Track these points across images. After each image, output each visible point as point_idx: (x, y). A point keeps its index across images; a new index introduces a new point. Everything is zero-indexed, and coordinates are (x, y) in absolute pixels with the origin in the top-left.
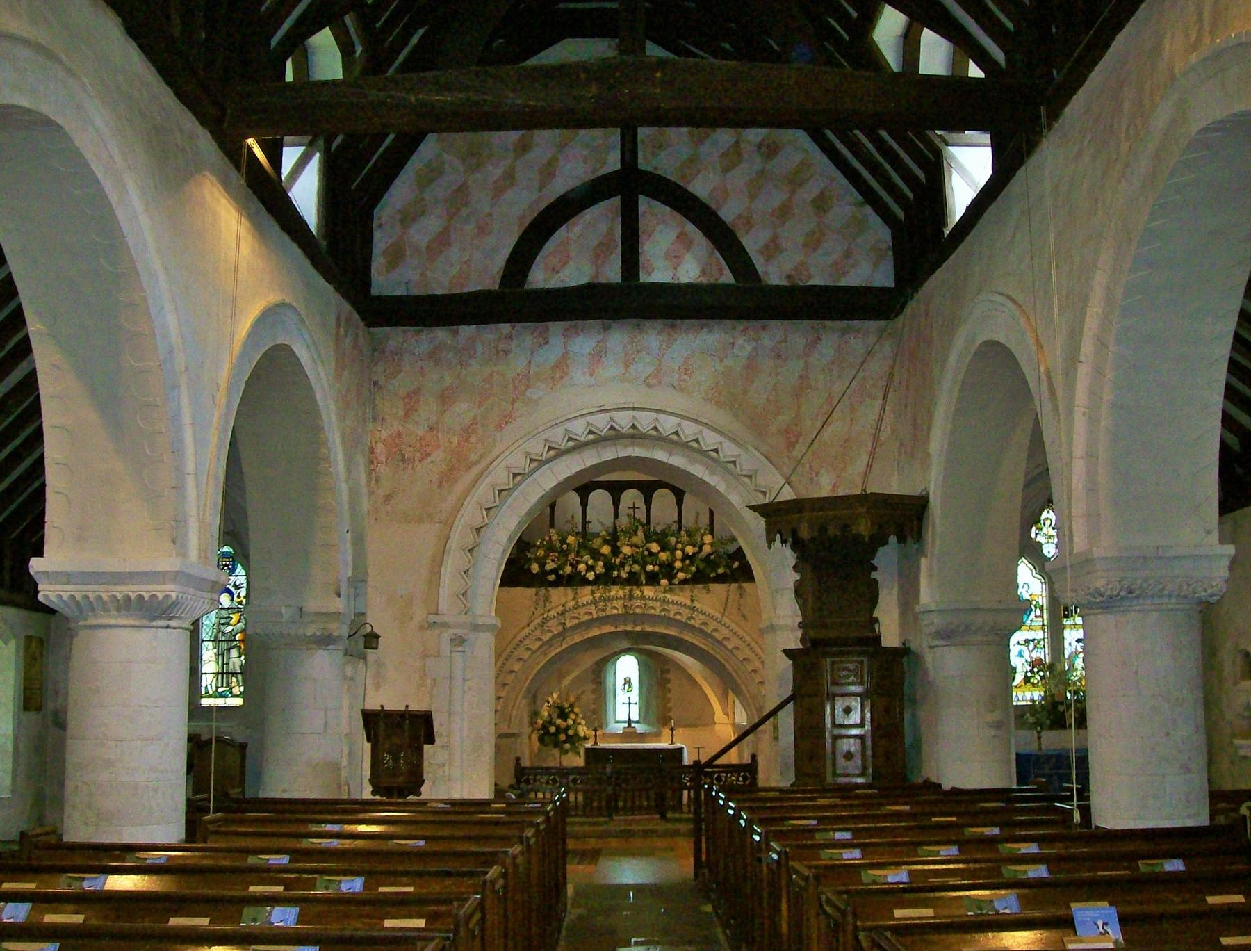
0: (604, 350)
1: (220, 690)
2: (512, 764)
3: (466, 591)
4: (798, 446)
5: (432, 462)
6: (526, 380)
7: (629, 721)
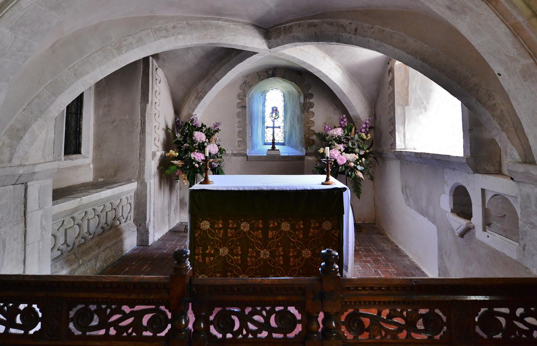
7: (273, 143)
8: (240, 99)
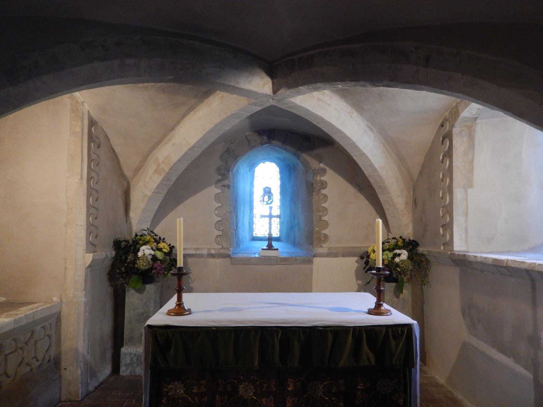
8: (220, 174)
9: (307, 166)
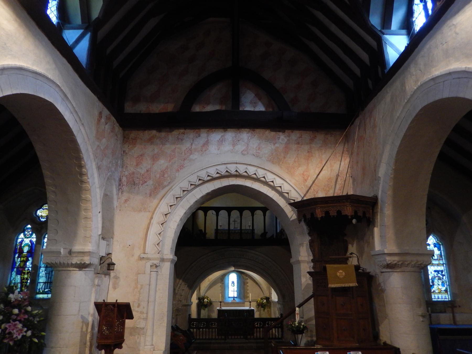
0: (224, 140)
1: (46, 290)
2: (187, 317)
3: (159, 243)
4: (308, 181)
5: (147, 185)
6: (190, 151)
8: (221, 280)
9: (243, 277)
